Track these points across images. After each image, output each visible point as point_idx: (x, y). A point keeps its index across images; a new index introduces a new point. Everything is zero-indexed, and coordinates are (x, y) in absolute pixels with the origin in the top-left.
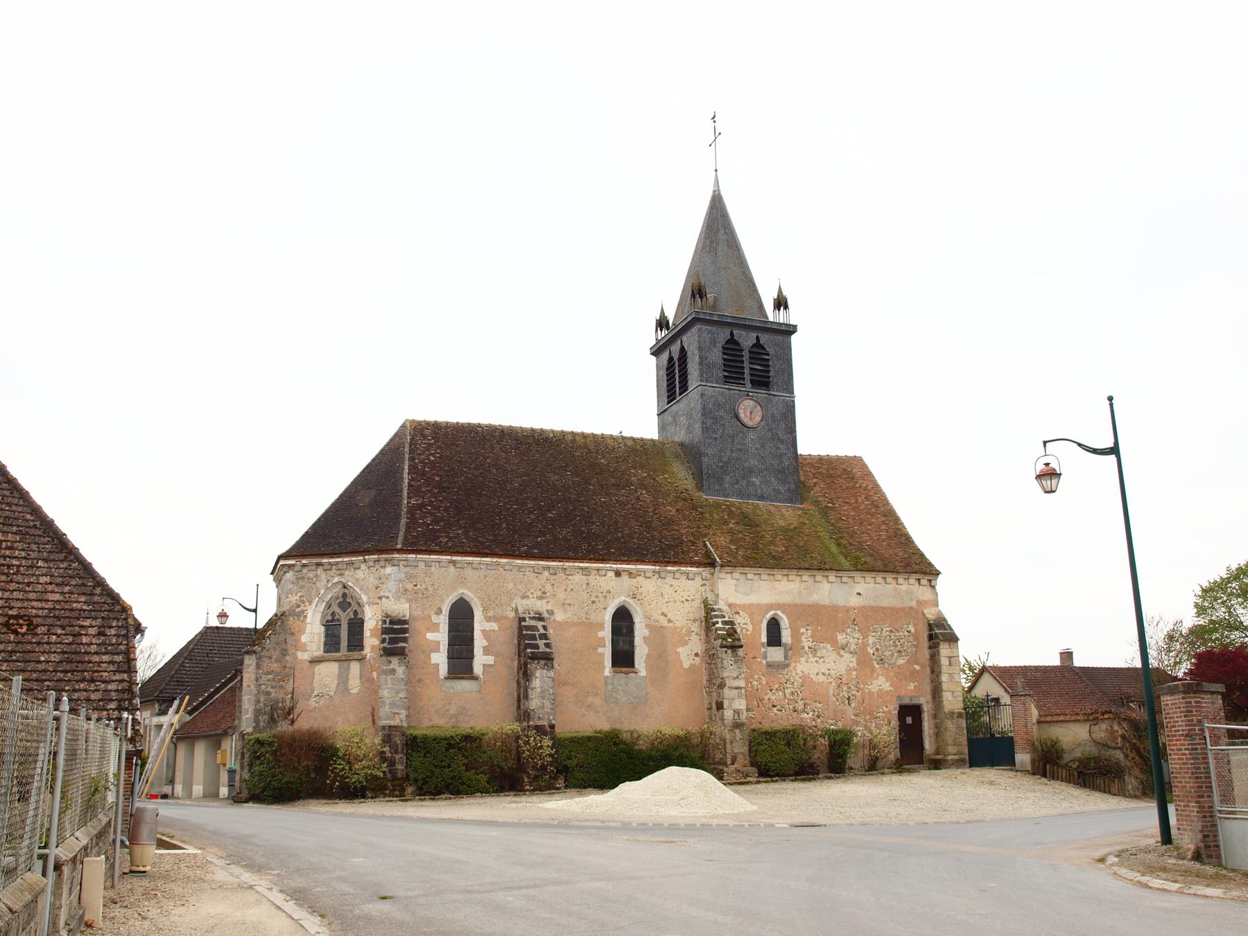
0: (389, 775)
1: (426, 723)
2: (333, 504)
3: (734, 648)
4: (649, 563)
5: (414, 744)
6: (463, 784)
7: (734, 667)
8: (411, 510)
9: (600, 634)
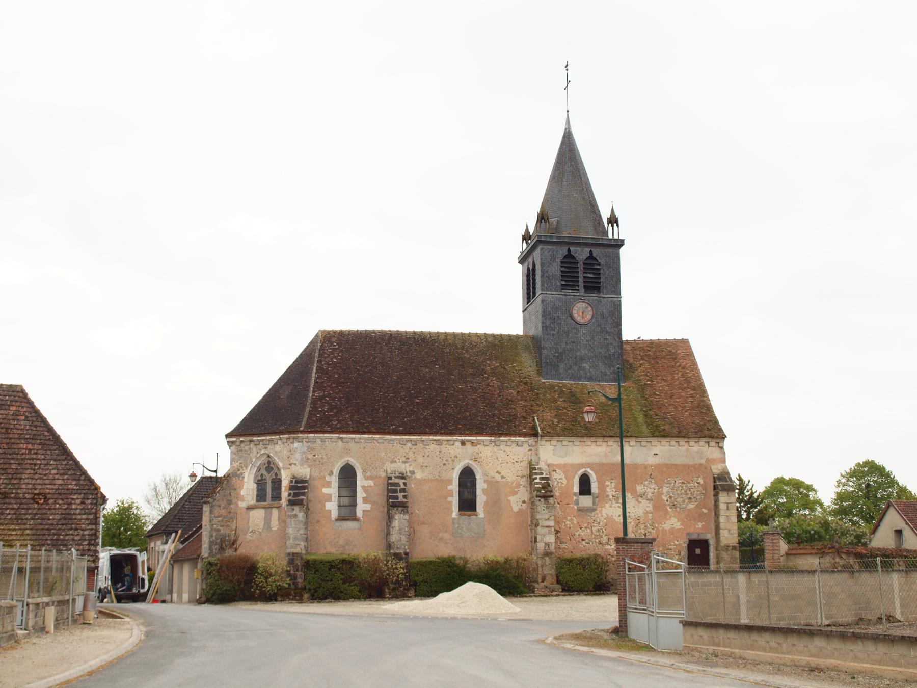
0: (293, 586)
1: (322, 551)
2: (264, 397)
3: (545, 497)
4: (486, 435)
5: (309, 565)
6: (342, 592)
7: (546, 511)
8: (314, 402)
9: (449, 487)
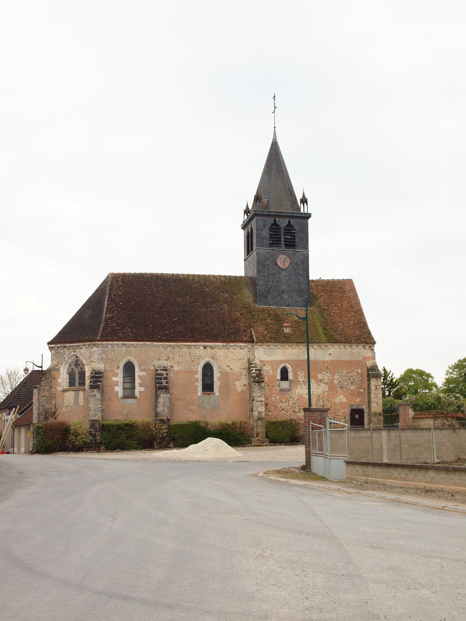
0: (93, 442)
1: (113, 418)
2: (73, 317)
3: (259, 382)
4: (220, 342)
5: (104, 428)
6: (126, 445)
7: (259, 391)
8: (107, 320)
9: (196, 376)
